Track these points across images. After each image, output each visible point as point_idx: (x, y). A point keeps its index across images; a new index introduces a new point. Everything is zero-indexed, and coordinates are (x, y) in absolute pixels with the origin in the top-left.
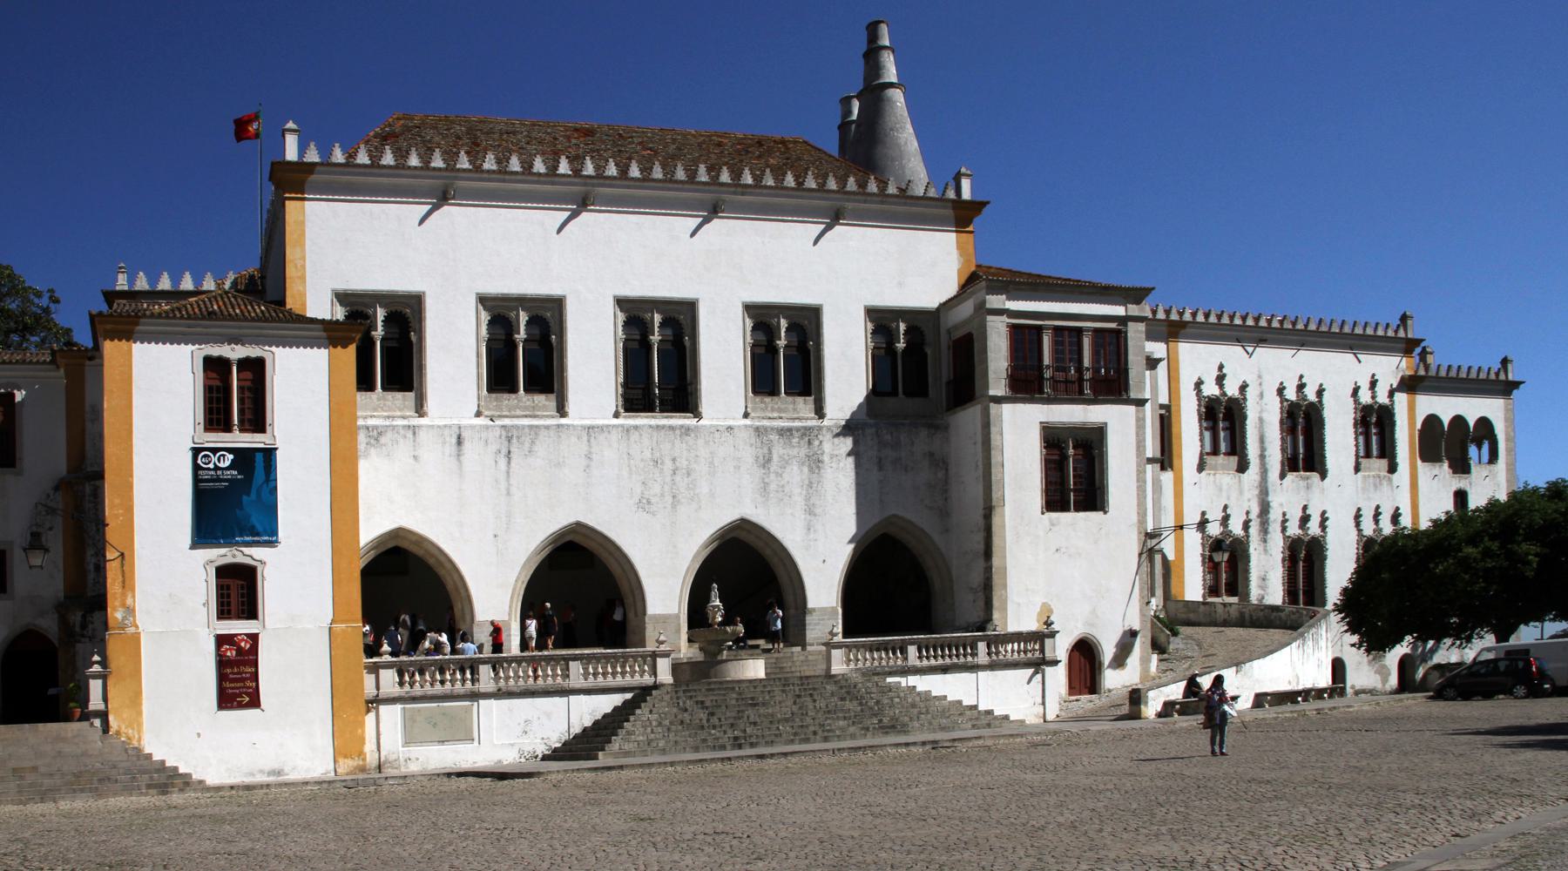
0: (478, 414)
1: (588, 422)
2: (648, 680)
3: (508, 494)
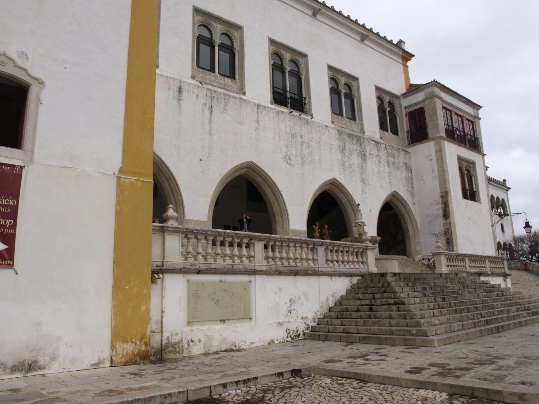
0: (193, 77)
1: (257, 102)
3: (210, 133)
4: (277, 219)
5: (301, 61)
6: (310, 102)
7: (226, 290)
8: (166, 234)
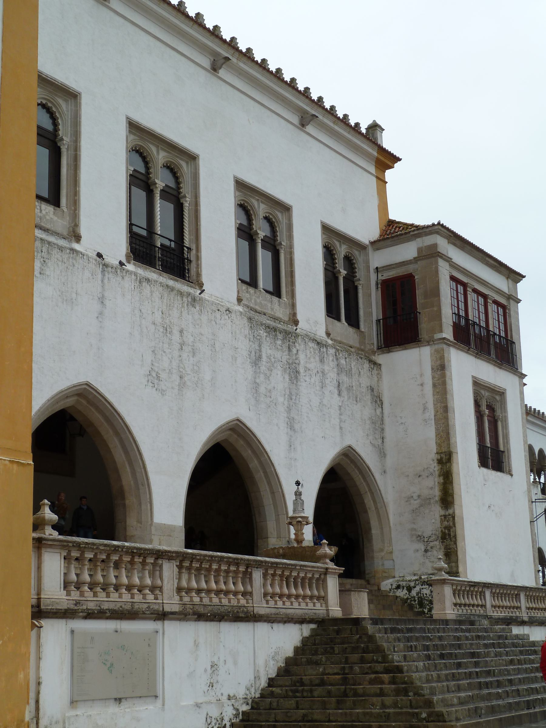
2: (317, 609)
4: (127, 502)
5: (185, 167)
6: (198, 258)
7: (123, 647)
8: (43, 550)
